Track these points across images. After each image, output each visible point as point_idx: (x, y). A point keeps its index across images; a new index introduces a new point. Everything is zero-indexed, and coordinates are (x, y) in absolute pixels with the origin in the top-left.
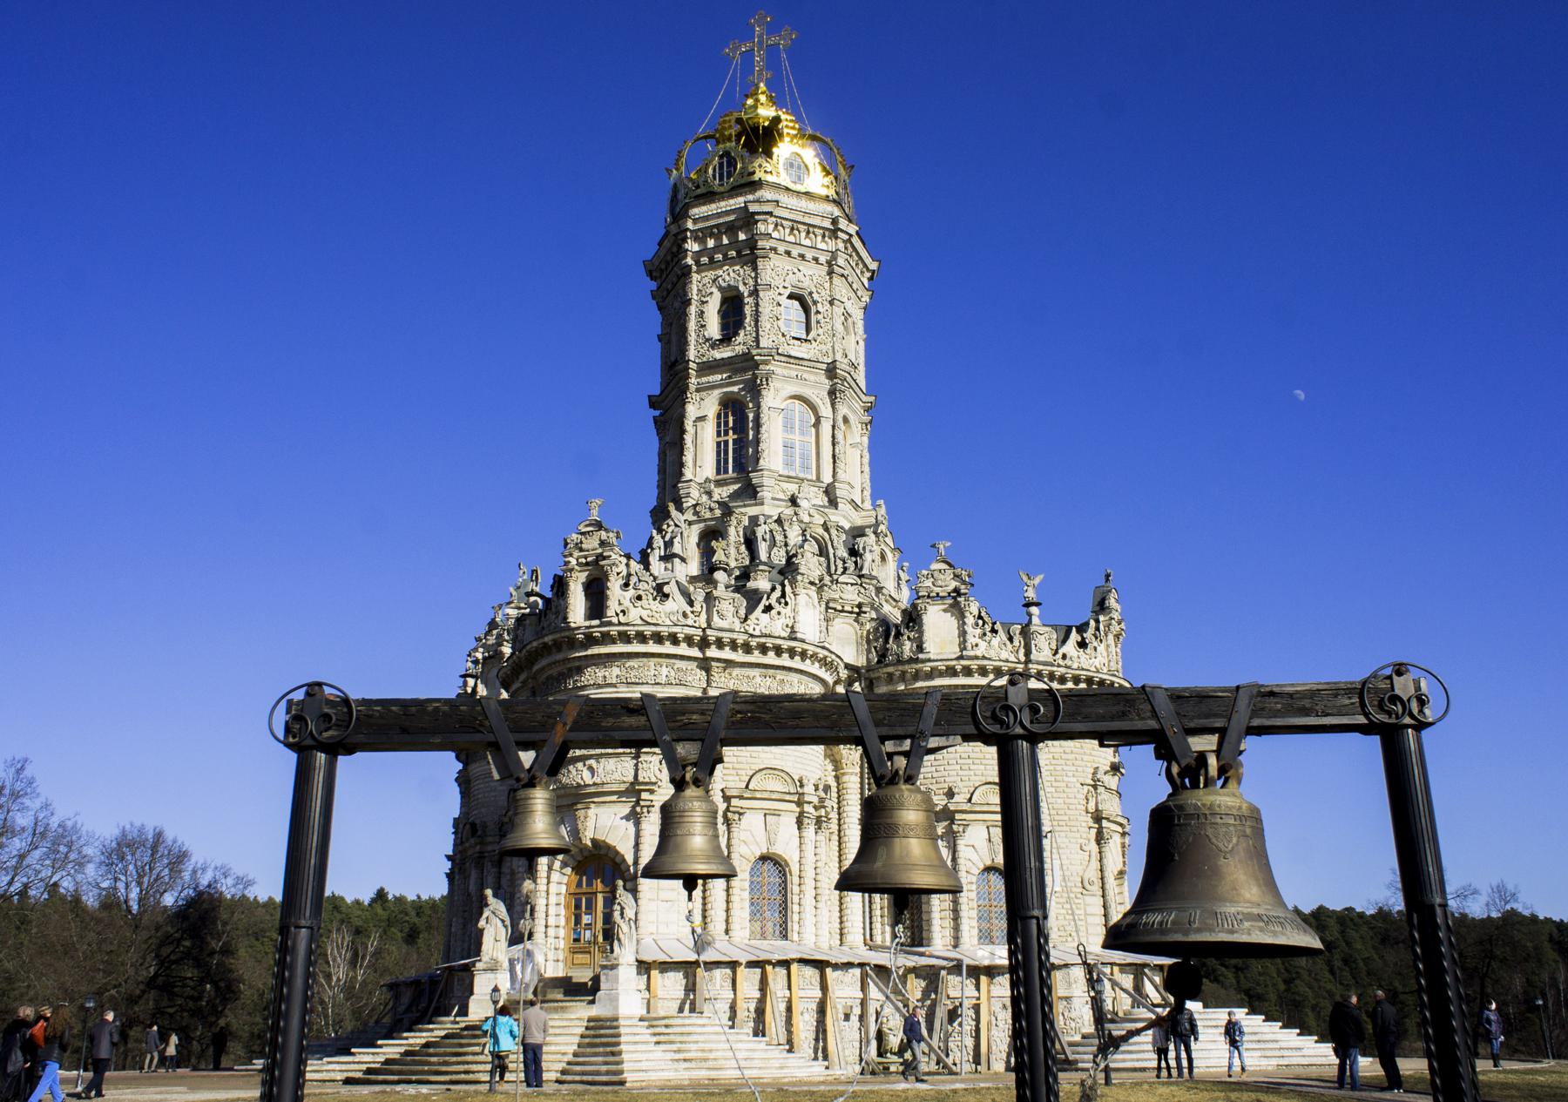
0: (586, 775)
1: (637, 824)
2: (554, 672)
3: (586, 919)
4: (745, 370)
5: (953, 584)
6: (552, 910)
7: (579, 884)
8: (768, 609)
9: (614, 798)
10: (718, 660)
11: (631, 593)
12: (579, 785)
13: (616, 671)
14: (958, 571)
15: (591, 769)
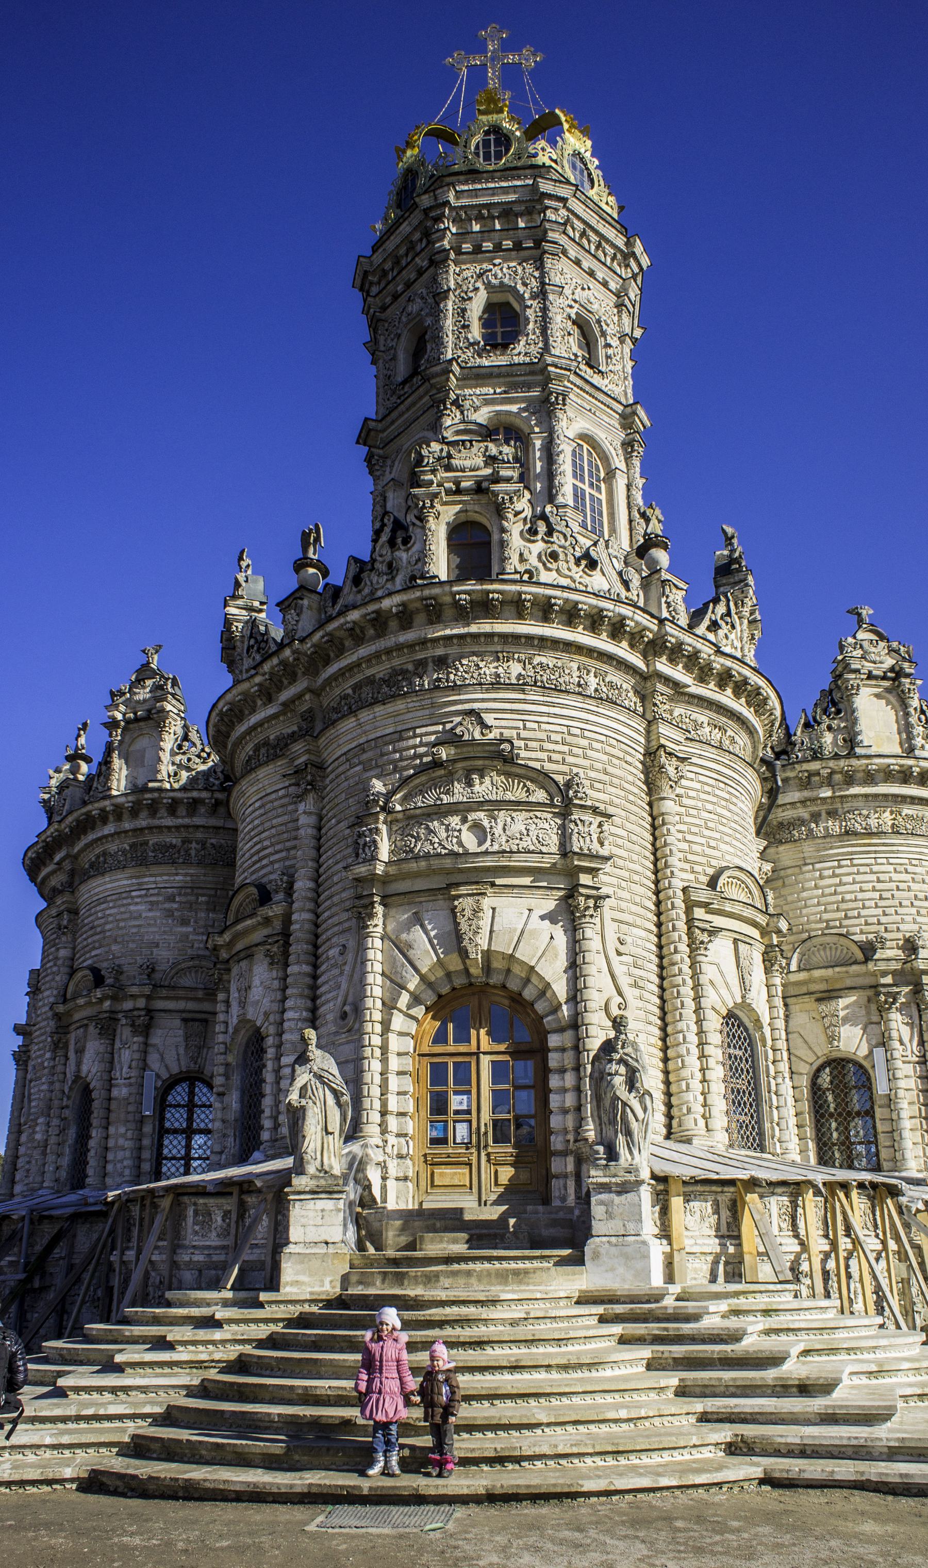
0: (470, 841)
1: (574, 929)
2: (379, 670)
3: (456, 1102)
4: (529, 386)
5: (890, 662)
6: (394, 1083)
7: (441, 1037)
8: (714, 626)
9: (526, 881)
10: (667, 680)
11: (539, 547)
12: (452, 854)
13: (516, 669)
14: (895, 644)
15: (477, 827)
